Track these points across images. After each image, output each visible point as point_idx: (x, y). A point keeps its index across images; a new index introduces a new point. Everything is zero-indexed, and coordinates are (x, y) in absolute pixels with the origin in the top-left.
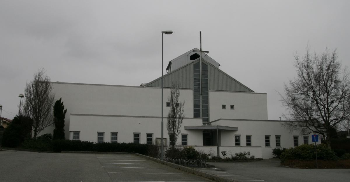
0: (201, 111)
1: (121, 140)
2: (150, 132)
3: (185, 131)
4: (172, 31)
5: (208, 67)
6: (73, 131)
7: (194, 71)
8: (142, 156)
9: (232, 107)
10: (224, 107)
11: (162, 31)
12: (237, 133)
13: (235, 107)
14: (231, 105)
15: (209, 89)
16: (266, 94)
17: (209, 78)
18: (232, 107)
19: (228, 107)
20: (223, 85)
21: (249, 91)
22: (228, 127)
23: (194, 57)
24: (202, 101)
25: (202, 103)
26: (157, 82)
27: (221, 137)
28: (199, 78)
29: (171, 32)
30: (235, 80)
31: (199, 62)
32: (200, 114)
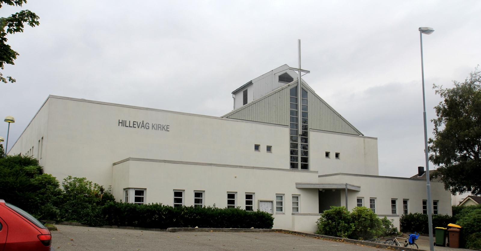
0: (300, 159)
1: (207, 203)
2: (250, 191)
3: (297, 190)
4: (432, 28)
5: (308, 94)
6: (134, 188)
7: (290, 98)
8: (242, 229)
9: (269, 149)
10: (257, 147)
11: (421, 27)
12: (359, 195)
13: (273, 149)
14: (255, 145)
15: (309, 128)
16: (376, 139)
17: (309, 111)
18: (269, 149)
19: (332, 155)
20: (327, 122)
21: (358, 134)
22: (353, 186)
23: (285, 78)
24: (301, 144)
25: (301, 147)
26: (241, 111)
27: (341, 199)
28: (296, 110)
29: (431, 29)
30: (340, 116)
31: (297, 87)
32: (298, 163)
